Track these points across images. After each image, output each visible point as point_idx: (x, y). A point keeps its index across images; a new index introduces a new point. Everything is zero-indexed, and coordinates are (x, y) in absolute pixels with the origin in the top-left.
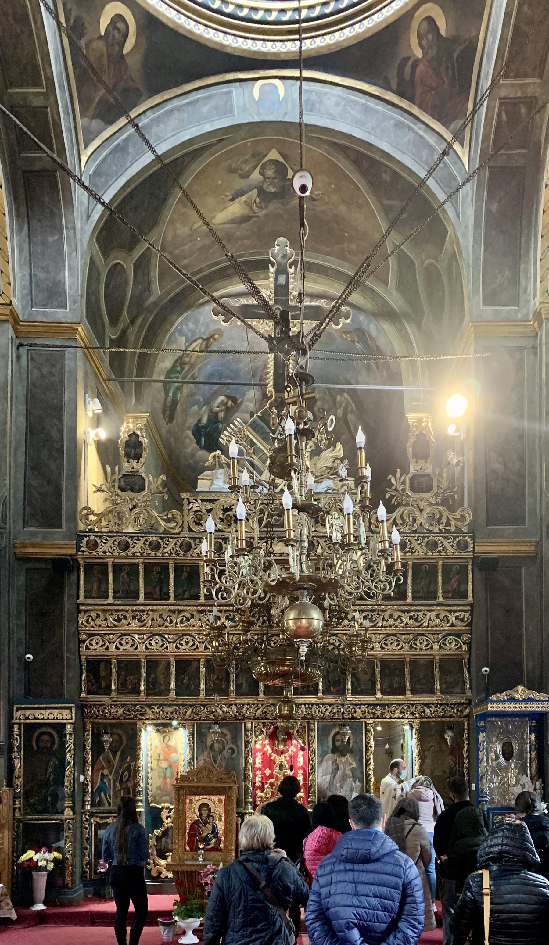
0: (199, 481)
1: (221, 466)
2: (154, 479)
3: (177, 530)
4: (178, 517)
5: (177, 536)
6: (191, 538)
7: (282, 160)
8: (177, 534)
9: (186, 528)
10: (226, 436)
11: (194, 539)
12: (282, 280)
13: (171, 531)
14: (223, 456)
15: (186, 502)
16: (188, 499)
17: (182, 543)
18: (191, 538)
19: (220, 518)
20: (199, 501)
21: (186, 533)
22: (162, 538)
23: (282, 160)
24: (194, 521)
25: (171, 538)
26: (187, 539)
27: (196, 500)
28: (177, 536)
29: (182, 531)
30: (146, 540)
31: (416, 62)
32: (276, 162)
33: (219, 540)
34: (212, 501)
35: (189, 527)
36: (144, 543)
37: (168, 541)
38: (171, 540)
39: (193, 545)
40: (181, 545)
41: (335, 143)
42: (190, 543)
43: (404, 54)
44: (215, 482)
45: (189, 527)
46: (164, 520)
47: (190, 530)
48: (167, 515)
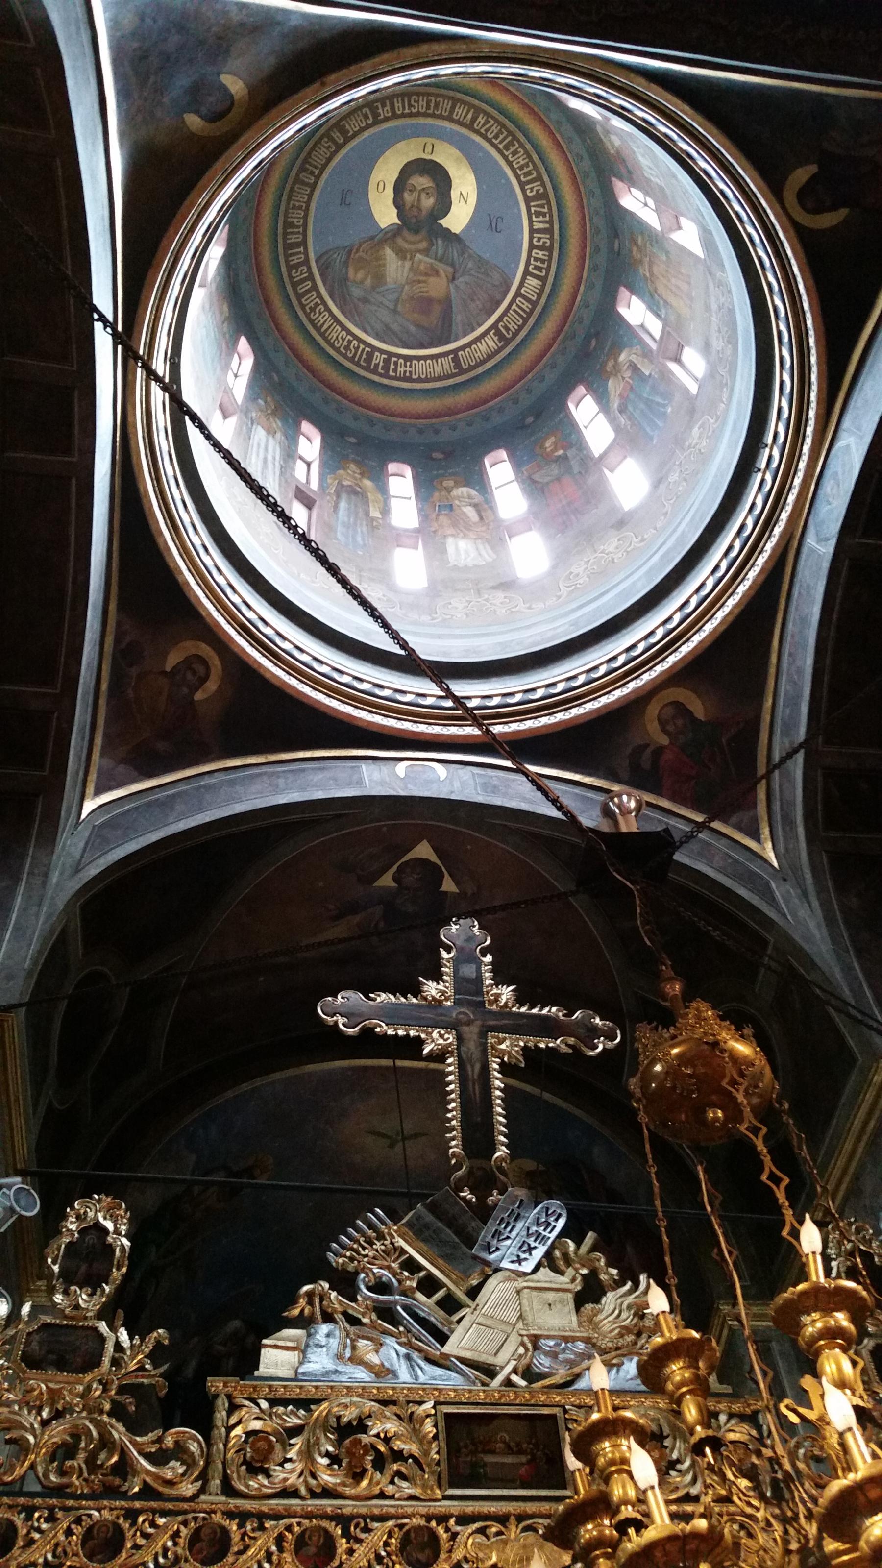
0: (263, 1351)
1: (328, 1318)
2: (131, 1338)
3: (188, 1489)
4: (193, 1447)
5: (186, 1506)
6: (230, 1515)
7: (434, 858)
8: (185, 1500)
9: (216, 1483)
10: (344, 1247)
11: (243, 1517)
12: (468, 971)
13: (166, 1490)
14: (334, 1294)
15: (222, 1404)
16: (229, 1397)
17: (197, 1531)
18: (230, 1515)
19: (328, 1454)
20: (264, 1405)
21: (214, 1499)
22: (132, 1515)
23: (434, 858)
24: (245, 1462)
25: (164, 1513)
26: (217, 1518)
27: (255, 1402)
28: (186, 1506)
29: (202, 1490)
30: (78, 1521)
31: (659, 751)
32: (424, 863)
33: (325, 1524)
34: (305, 1404)
35: (226, 1481)
36: (69, 1532)
37: (153, 1524)
38: (161, 1521)
39: (236, 1537)
40: (195, 1539)
41: (534, 835)
42: (225, 1532)
43: (638, 741)
44: (311, 1356)
45: (226, 1481)
46: (148, 1456)
47: (228, 1490)
48: (160, 1440)
